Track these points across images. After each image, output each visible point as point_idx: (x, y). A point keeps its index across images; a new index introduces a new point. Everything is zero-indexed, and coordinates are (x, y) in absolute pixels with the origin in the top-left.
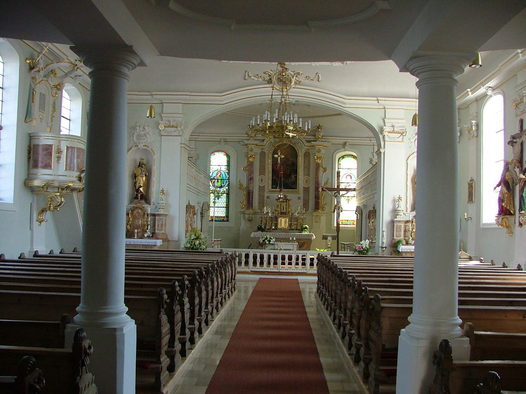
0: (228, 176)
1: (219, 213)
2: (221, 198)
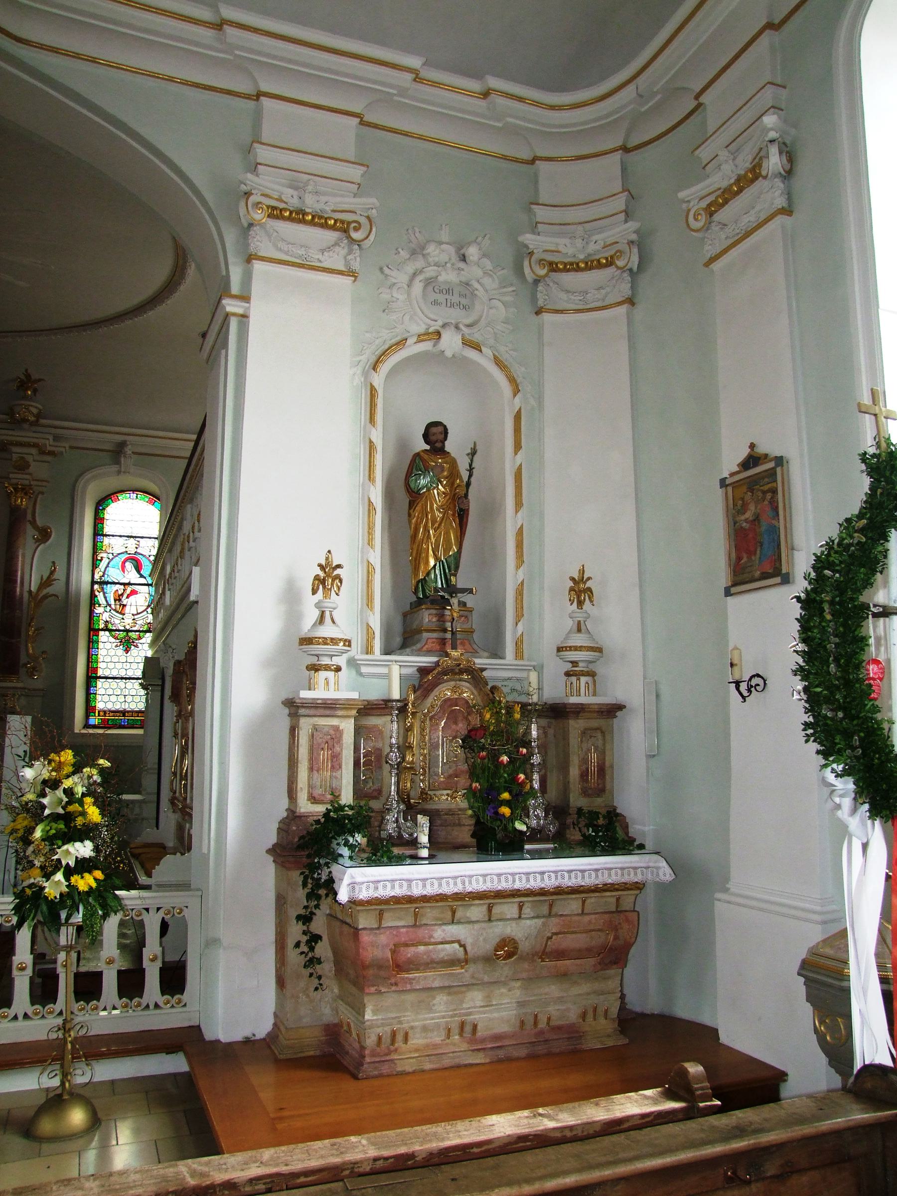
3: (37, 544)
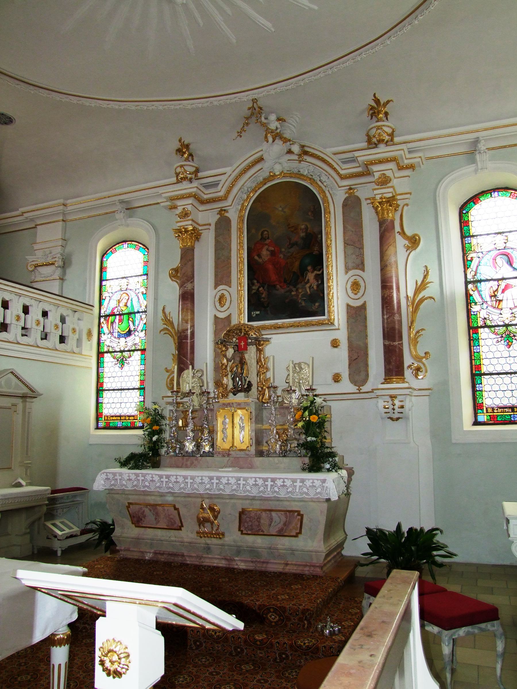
1: (123, 405)
3: (408, 251)
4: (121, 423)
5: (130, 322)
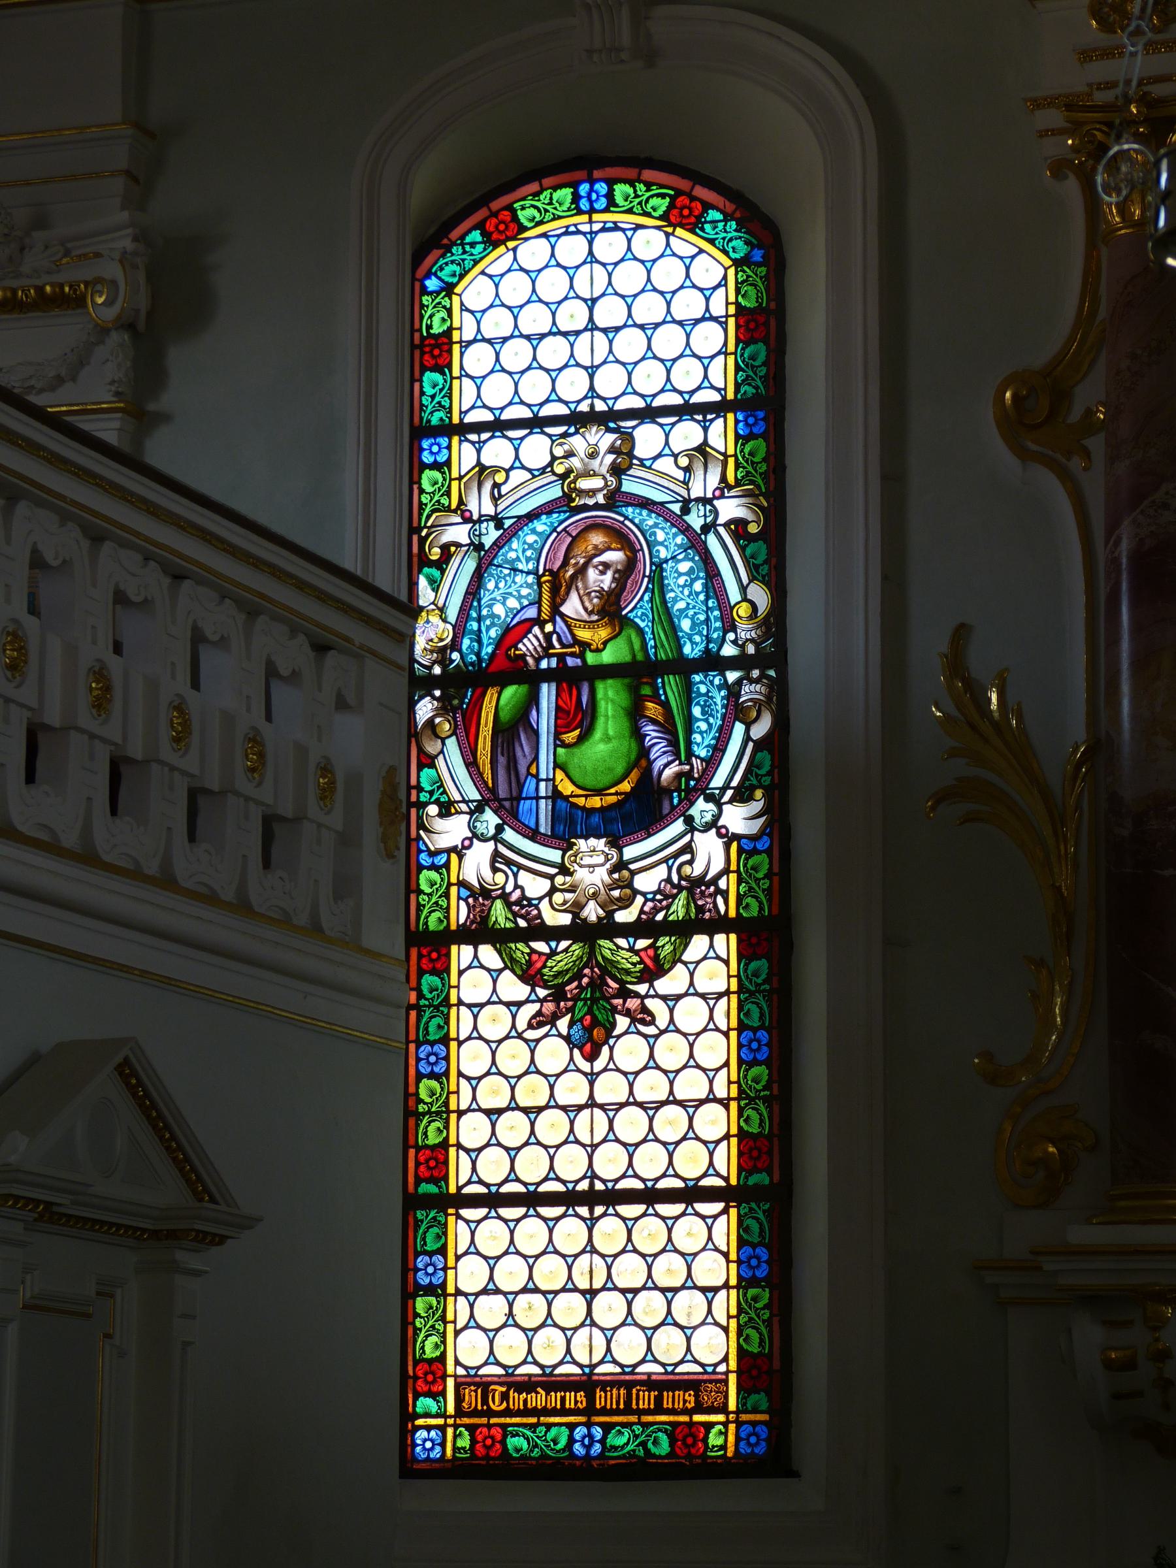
0: (760, 595)
1: (609, 1308)
2: (643, 1017)
4: (598, 1432)
5: (649, 730)
